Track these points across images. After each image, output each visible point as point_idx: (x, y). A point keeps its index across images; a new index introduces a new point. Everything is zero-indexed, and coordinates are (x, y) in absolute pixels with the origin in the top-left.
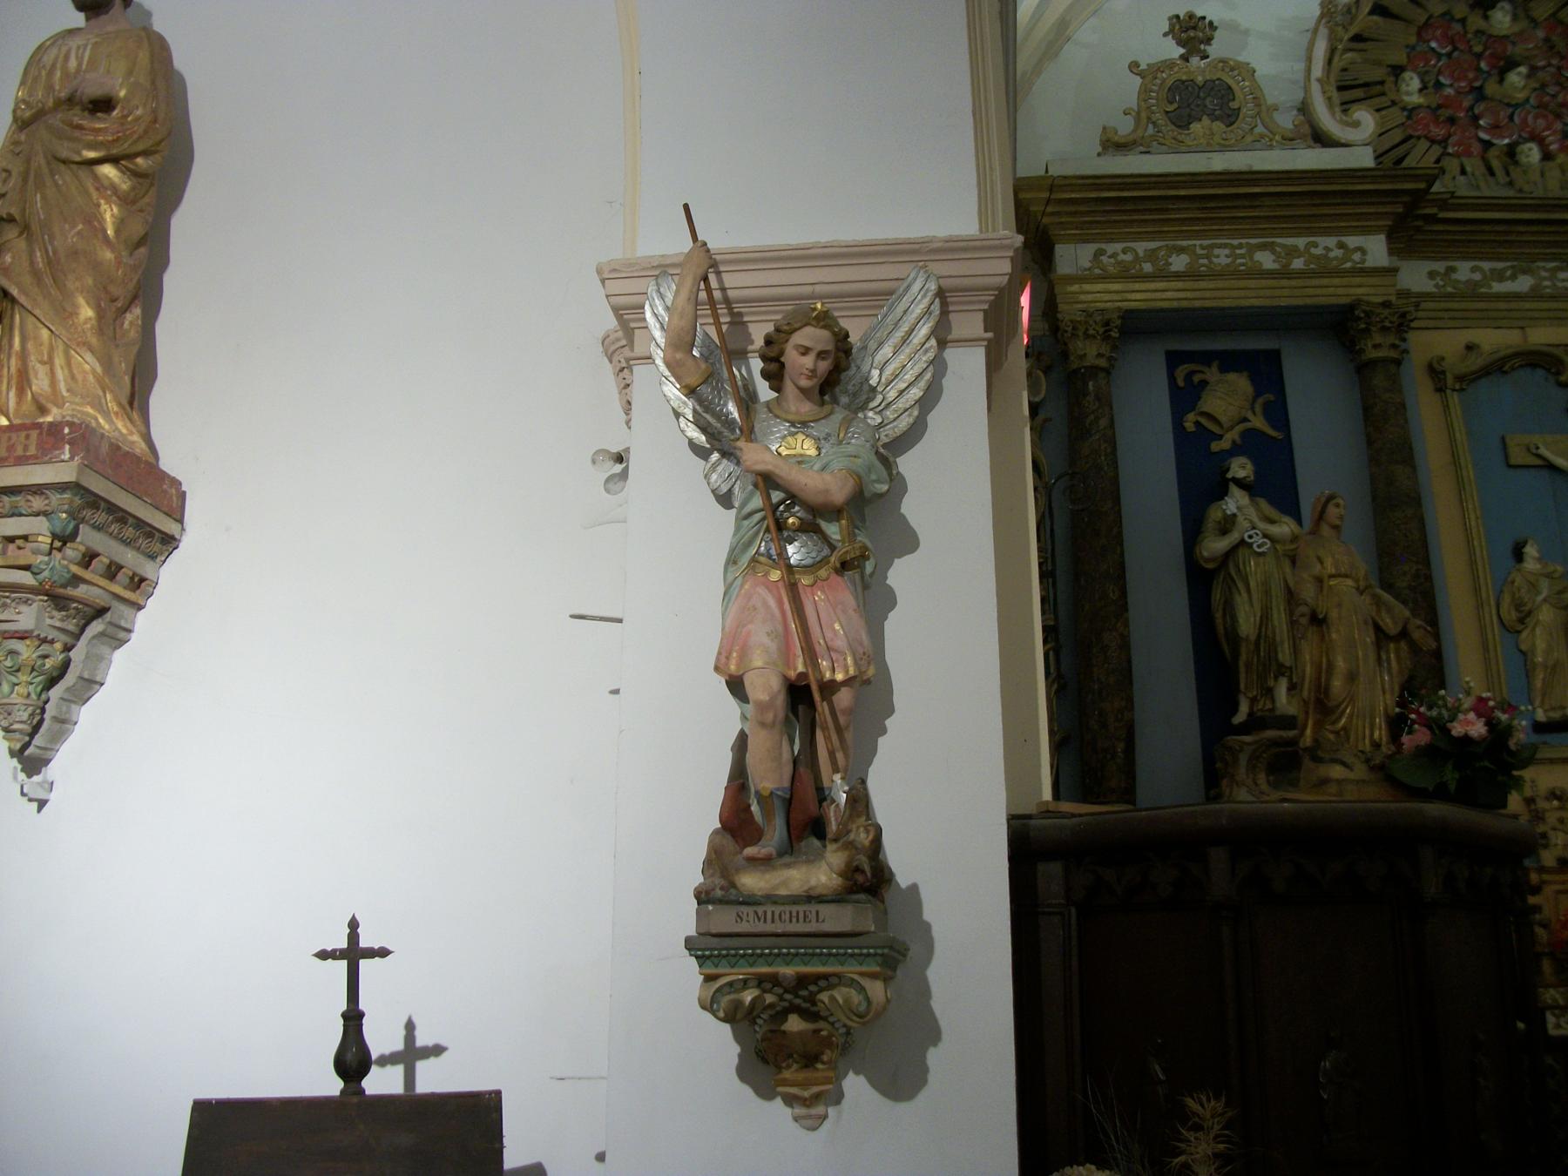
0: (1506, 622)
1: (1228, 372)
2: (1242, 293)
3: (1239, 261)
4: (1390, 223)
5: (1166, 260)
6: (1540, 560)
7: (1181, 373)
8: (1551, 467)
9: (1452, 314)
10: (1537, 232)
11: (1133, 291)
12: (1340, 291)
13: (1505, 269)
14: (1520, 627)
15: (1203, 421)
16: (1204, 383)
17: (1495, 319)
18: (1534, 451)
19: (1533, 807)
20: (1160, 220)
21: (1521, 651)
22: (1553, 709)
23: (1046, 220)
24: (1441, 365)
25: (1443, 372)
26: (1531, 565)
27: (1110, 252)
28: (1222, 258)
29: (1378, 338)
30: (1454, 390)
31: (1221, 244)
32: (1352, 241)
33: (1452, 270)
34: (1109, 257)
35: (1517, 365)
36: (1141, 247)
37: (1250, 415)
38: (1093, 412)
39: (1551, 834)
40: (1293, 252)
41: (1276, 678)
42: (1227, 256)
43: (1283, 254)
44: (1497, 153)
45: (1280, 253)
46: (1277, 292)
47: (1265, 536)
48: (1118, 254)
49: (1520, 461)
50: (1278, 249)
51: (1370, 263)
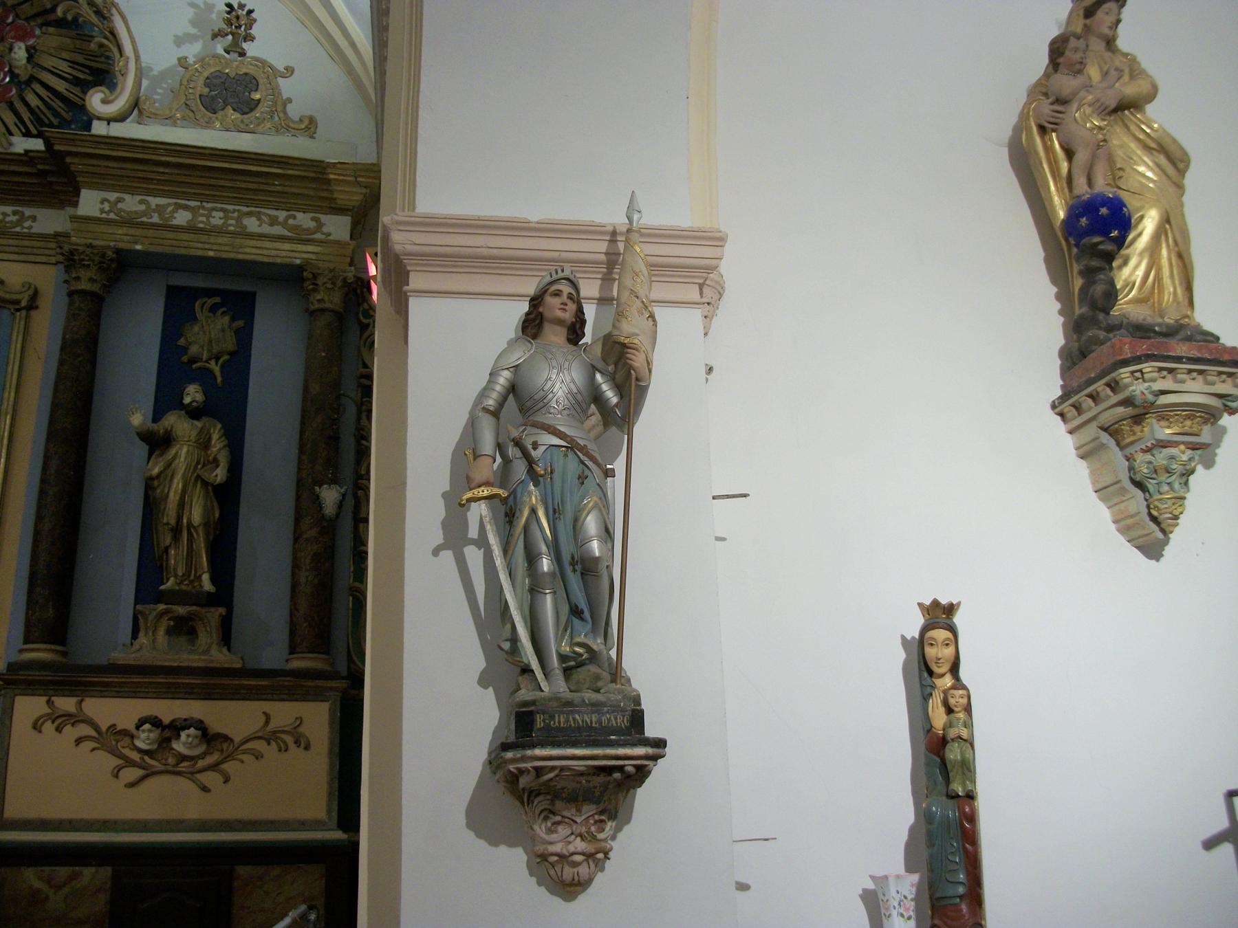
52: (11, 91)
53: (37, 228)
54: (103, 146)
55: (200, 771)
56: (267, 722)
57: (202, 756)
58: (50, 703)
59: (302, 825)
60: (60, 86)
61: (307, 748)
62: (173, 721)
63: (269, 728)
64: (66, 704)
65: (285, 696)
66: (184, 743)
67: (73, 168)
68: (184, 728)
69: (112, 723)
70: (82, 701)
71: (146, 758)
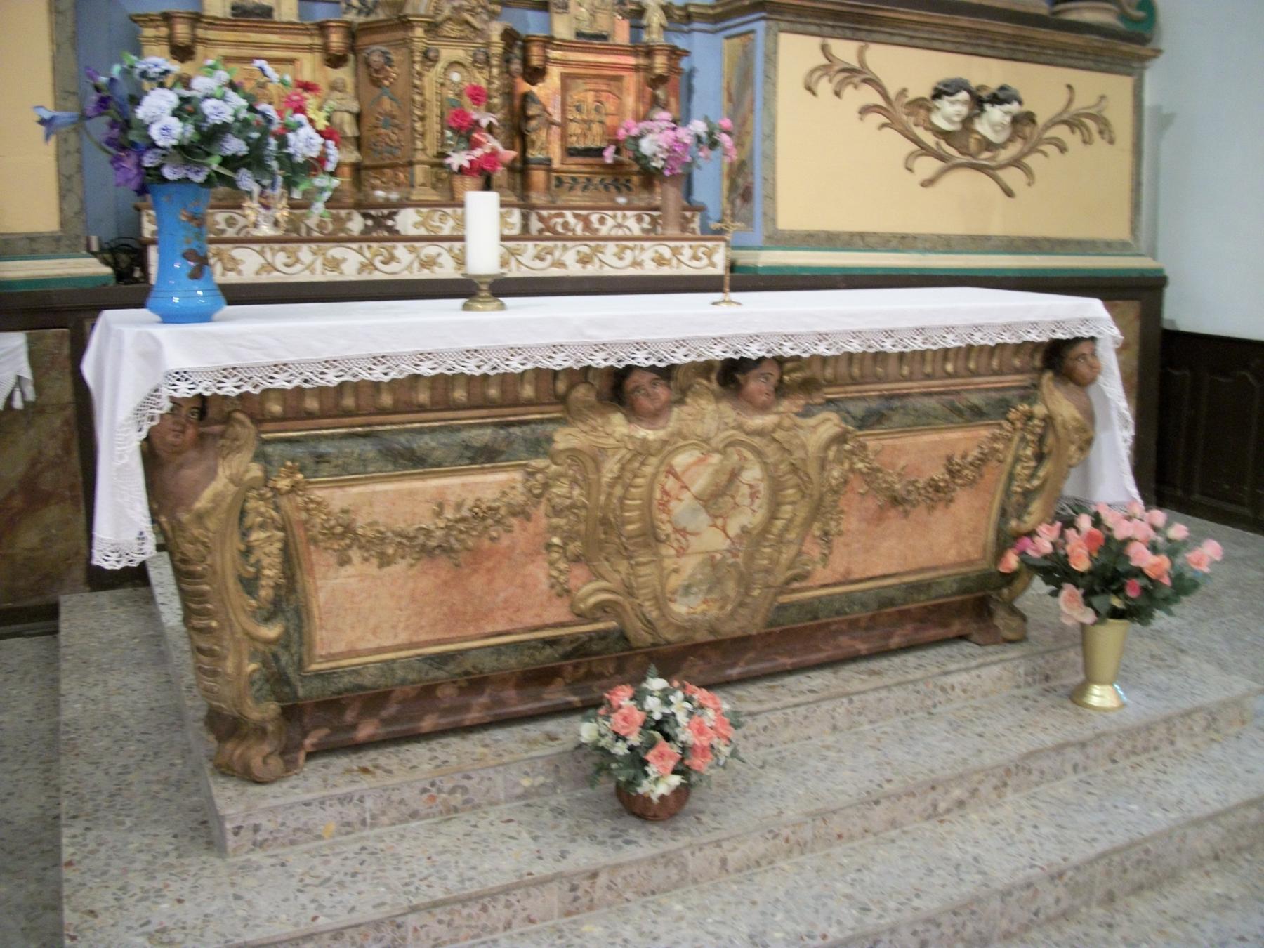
55: (1002, 167)
56: (1070, 101)
57: (1003, 146)
58: (824, 49)
59: (1107, 247)
61: (1111, 142)
62: (982, 87)
63: (1076, 107)
64: (845, 50)
65: (1091, 64)
66: (994, 119)
68: (996, 99)
69: (903, 86)
70: (867, 47)
71: (943, 144)
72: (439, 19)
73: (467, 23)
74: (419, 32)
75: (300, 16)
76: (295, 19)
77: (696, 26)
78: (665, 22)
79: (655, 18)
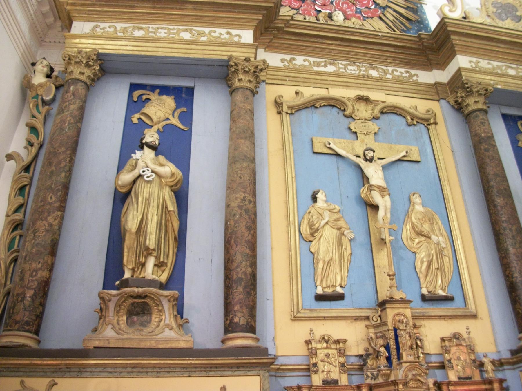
0: (303, 236)
1: (163, 95)
2: (170, 50)
3: (171, 36)
4: (256, 24)
5: (132, 32)
6: (326, 201)
7: (136, 94)
8: (338, 155)
9: (291, 79)
10: (336, 45)
11: (109, 45)
12: (224, 53)
13: (322, 62)
14: (311, 238)
15: (143, 118)
16: (148, 100)
17: (314, 83)
18: (328, 146)
19: (310, 346)
20: (131, 12)
21: (311, 252)
22: (328, 287)
23: (68, 8)
24: (280, 99)
25: (282, 104)
26: (321, 202)
27: (101, 27)
28: (162, 33)
29: (241, 77)
30: (287, 113)
31: (163, 27)
32: (234, 32)
33: (294, 59)
34: (101, 29)
35: (322, 105)
36: (119, 26)
37: (171, 117)
38: (68, 101)
39: (320, 365)
40: (200, 34)
41: (146, 258)
42: (165, 33)
43: (196, 34)
44: (323, 15)
45: (195, 34)
46: (189, 51)
47: (153, 172)
48: (106, 28)
49: (320, 151)
50: (194, 32)
51: (243, 41)
52: (378, 11)
53: (420, 80)
54: (473, 29)
60: (402, 11)
67: (454, 42)
72: (408, 380)
73: (419, 380)
74: (401, 386)
75: (349, 383)
76: (347, 384)
77: (505, 367)
78: (493, 368)
79: (489, 367)
